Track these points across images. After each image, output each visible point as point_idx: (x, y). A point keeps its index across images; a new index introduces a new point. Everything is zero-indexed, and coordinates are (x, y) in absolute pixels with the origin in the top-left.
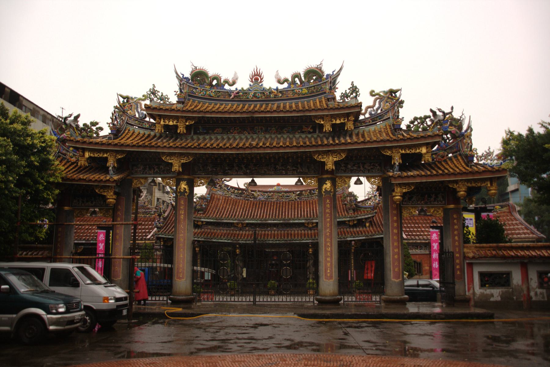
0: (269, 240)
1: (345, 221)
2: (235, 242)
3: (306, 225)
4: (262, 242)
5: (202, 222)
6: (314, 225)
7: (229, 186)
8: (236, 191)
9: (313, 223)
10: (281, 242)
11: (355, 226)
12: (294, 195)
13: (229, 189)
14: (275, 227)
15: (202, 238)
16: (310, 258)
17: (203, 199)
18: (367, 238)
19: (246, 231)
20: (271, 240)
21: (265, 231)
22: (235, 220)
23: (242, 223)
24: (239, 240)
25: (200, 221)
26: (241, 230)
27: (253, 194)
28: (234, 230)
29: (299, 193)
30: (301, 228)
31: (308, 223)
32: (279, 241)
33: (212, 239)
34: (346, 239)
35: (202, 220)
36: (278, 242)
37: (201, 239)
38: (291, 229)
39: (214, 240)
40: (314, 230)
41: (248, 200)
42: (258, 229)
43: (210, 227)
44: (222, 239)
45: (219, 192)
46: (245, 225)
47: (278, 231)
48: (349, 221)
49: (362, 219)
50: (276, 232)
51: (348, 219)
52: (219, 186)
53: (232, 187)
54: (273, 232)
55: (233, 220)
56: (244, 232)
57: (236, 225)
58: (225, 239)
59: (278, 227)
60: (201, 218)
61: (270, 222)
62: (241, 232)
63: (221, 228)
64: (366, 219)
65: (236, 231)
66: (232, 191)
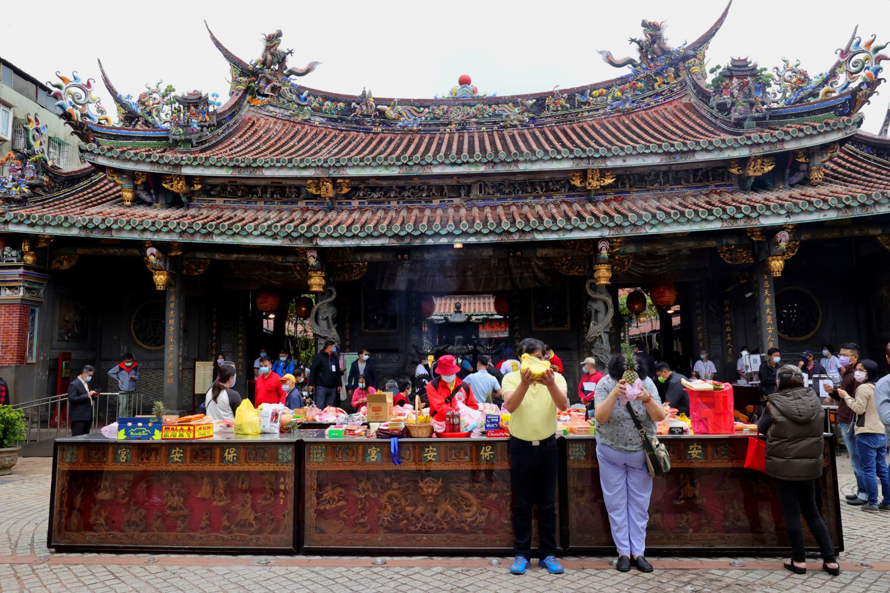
0: (437, 234)
1: (728, 162)
2: (300, 244)
3: (577, 183)
4: (407, 241)
5: (189, 180)
6: (609, 181)
7: (305, 89)
8: (326, 103)
9: (603, 173)
10: (485, 240)
11: (760, 185)
12: (516, 110)
13: (305, 99)
14: (459, 196)
15: (170, 231)
16: (599, 306)
17: (196, 106)
18: (841, 216)
19: (351, 211)
20: (443, 232)
21: (422, 210)
22: (306, 168)
23: (334, 180)
24: (316, 236)
25: (181, 177)
26: (331, 209)
27: (382, 113)
28: (308, 210)
29: (535, 103)
30: (558, 198)
31: (584, 174)
32: (477, 233)
33: (210, 234)
34: (754, 224)
35: (187, 171)
36: (472, 240)
37: (167, 238)
38: (520, 202)
39: (218, 240)
40: (607, 202)
41: (367, 131)
42: (394, 204)
43: (219, 201)
44: (249, 234)
45: (272, 109)
46: (346, 190)
47: (469, 210)
48: (743, 162)
49: (794, 153)
50: (463, 212)
51: (744, 153)
52: (274, 89)
53: (314, 93)
54: (451, 211)
55: (299, 168)
56: (344, 215)
57: (313, 191)
58: (262, 234)
59: (468, 194)
60: (178, 166)
61: (437, 170)
62: (332, 215)
63: (261, 204)
64: (810, 153)
65: (316, 212)
66: (315, 104)
